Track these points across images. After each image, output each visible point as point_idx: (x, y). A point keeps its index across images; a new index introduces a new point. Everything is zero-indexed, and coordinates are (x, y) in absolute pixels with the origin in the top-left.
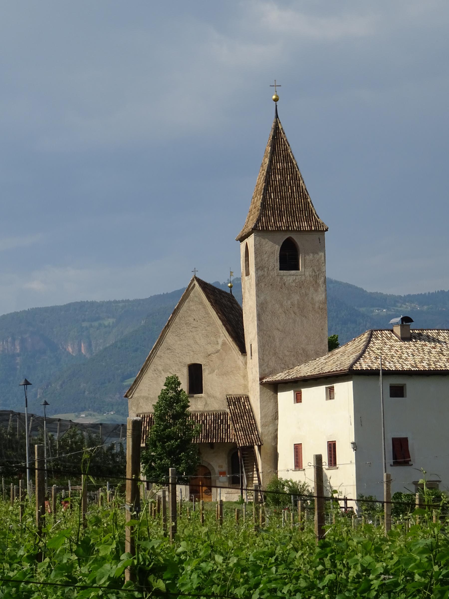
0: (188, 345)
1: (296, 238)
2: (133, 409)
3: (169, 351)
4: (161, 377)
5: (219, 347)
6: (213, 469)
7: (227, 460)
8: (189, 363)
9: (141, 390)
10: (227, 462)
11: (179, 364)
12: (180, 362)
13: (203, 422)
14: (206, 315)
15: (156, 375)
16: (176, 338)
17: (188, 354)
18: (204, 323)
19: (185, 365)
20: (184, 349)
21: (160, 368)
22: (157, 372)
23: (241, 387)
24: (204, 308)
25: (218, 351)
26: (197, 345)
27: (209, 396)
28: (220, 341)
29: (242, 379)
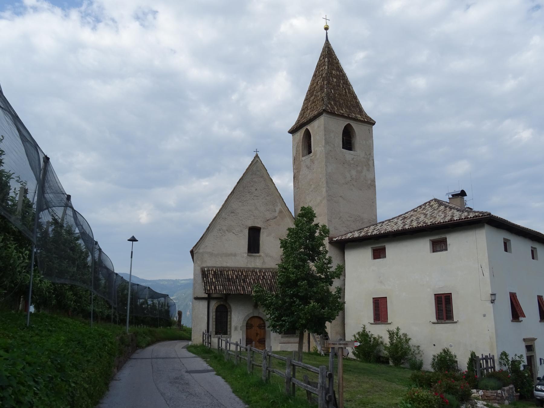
1: (354, 125)
3: (233, 214)
5: (276, 214)
9: (206, 246)
13: (263, 277)
16: (240, 204)
21: (224, 228)
25: (275, 218)
28: (278, 209)
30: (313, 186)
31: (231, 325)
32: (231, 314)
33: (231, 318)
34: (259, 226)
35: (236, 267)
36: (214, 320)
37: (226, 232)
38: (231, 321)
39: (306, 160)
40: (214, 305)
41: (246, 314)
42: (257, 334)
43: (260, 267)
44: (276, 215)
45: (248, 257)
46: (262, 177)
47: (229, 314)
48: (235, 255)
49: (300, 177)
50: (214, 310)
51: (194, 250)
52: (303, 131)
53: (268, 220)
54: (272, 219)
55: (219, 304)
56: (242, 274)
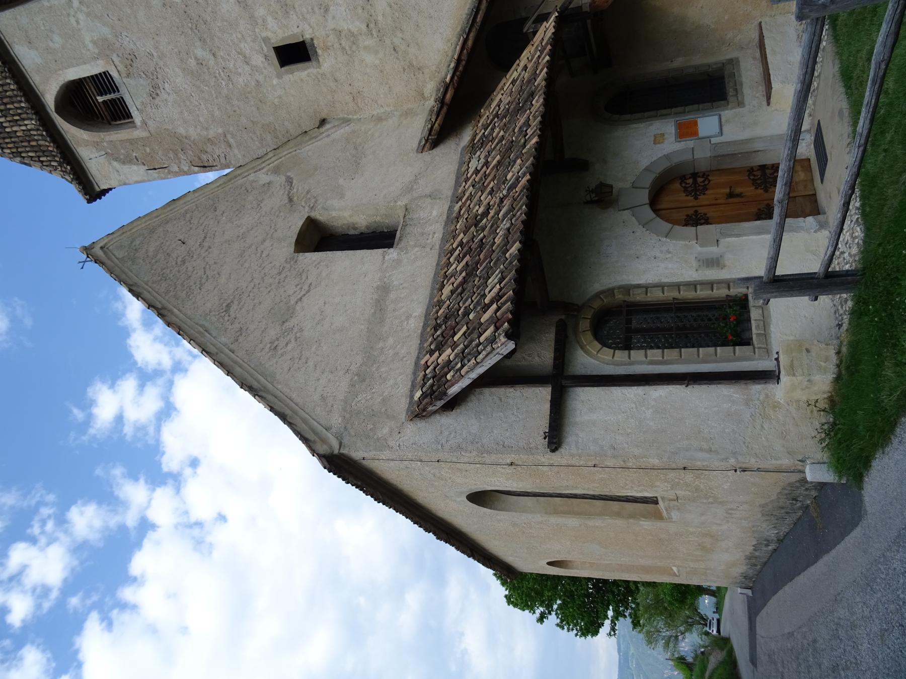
2: (386, 431)
3: (234, 307)
4: (301, 330)
6: (667, 157)
8: (292, 249)
10: (642, 125)
11: (283, 275)
12: (280, 273)
15: (290, 347)
17: (264, 255)
20: (247, 265)
21: (273, 333)
22: (282, 343)
27: (409, 189)
29: (384, 123)
30: (200, 53)
31: (694, 285)
33: (662, 286)
36: (671, 354)
38: (678, 286)
39: (133, 94)
40: (590, 358)
41: (640, 230)
42: (731, 195)
44: (283, 178)
46: (152, 231)
47: (639, 297)
49: (193, 133)
50: (621, 355)
51: (323, 449)
52: (73, 133)
53: (291, 200)
55: (587, 338)
56: (467, 250)
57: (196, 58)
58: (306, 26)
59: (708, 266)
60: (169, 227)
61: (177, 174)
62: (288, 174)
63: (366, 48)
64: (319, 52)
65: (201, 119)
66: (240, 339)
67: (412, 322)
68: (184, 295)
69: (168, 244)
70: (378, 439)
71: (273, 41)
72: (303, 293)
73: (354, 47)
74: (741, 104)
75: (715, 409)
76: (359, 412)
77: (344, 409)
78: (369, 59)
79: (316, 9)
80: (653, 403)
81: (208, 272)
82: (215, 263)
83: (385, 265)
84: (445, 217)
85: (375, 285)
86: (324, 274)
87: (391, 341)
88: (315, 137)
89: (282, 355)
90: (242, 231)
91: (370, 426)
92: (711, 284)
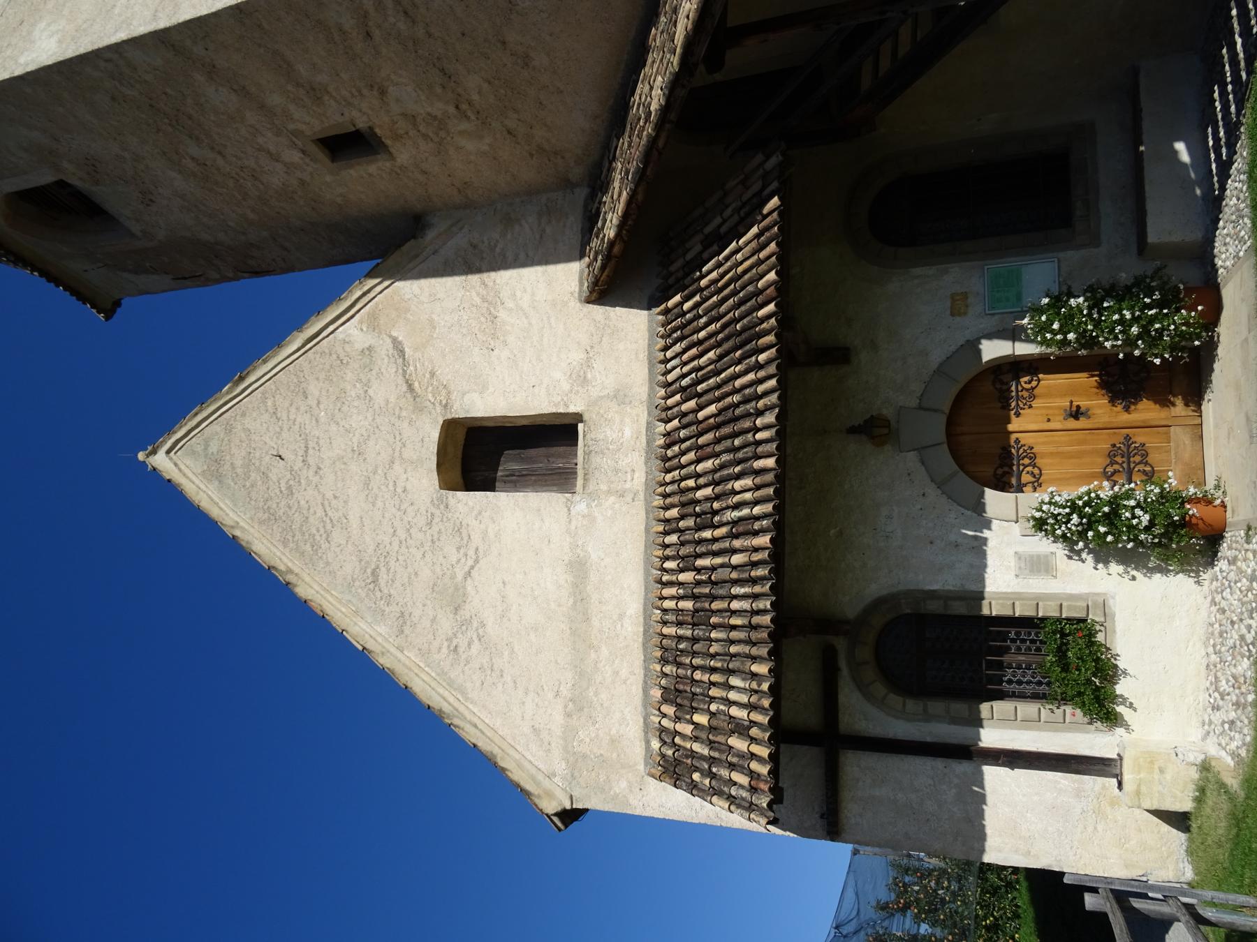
0: (367, 484)
3: (383, 577)
7: (917, 271)
10: (931, 271)
11: (435, 528)
12: (430, 524)
14: (269, 403)
16: (337, 537)
17: (399, 490)
18: (293, 410)
19: (440, 499)
20: (379, 504)
23: (548, 230)
24: (244, 415)
26: (371, 443)
32: (933, 595)
34: (435, 434)
35: (647, 562)
37: (465, 613)
41: (932, 492)
43: (644, 417)
44: (389, 341)
45: (592, 486)
47: (934, 607)
48: (579, 568)
53: (410, 387)
54: (405, 363)
57: (193, 159)
58: (355, 113)
59: (1032, 571)
60: (248, 422)
61: (218, 281)
62: (394, 334)
63: (461, 133)
64: (388, 142)
65: (231, 224)
66: (407, 630)
67: (627, 623)
68: (308, 548)
69: (257, 455)
70: (617, 795)
71: (308, 133)
72: (470, 562)
73: (443, 134)
74: (1095, 241)
75: (1036, 798)
76: (585, 756)
77: (565, 749)
78: (470, 145)
79: (365, 92)
80: (956, 781)
81: (330, 513)
82: (335, 497)
83: (574, 523)
84: (644, 441)
85: (566, 558)
86: (491, 534)
87: (605, 651)
88: (417, 256)
89: (468, 662)
90: (355, 440)
91: (602, 778)
92: (1037, 600)
